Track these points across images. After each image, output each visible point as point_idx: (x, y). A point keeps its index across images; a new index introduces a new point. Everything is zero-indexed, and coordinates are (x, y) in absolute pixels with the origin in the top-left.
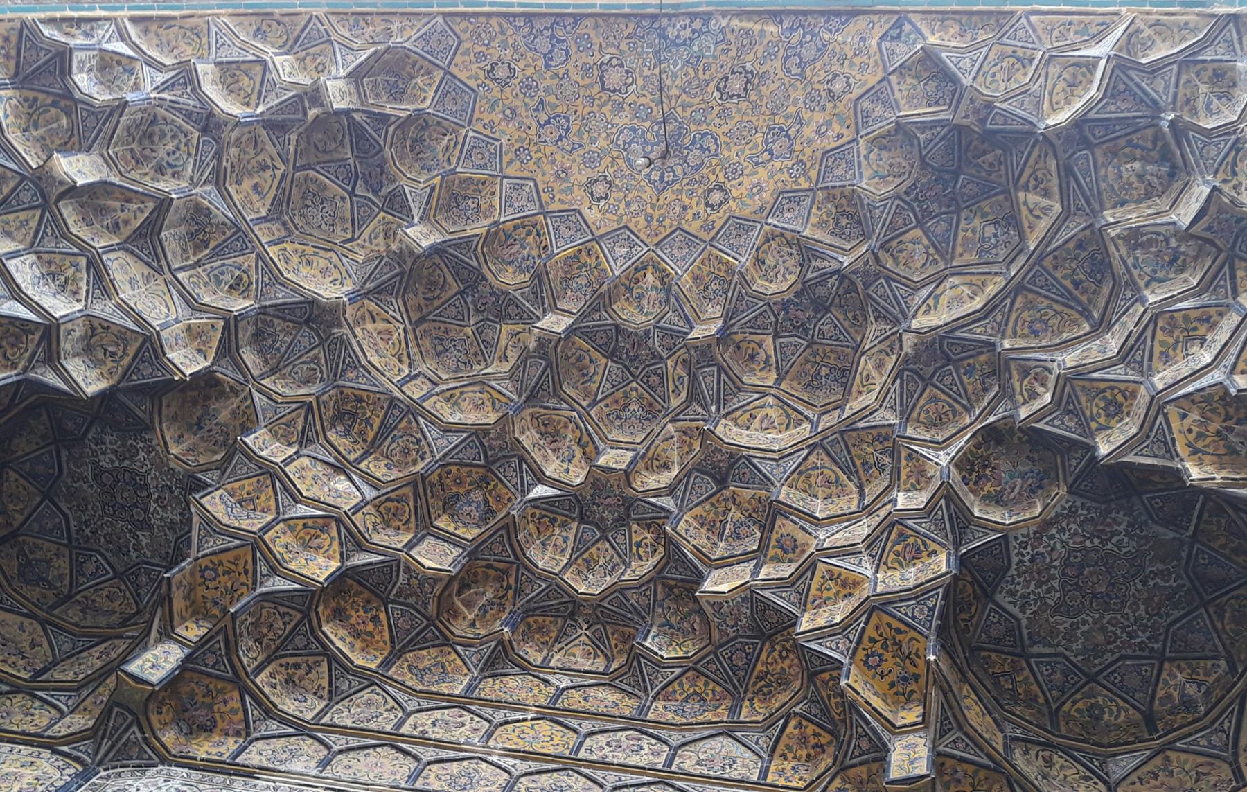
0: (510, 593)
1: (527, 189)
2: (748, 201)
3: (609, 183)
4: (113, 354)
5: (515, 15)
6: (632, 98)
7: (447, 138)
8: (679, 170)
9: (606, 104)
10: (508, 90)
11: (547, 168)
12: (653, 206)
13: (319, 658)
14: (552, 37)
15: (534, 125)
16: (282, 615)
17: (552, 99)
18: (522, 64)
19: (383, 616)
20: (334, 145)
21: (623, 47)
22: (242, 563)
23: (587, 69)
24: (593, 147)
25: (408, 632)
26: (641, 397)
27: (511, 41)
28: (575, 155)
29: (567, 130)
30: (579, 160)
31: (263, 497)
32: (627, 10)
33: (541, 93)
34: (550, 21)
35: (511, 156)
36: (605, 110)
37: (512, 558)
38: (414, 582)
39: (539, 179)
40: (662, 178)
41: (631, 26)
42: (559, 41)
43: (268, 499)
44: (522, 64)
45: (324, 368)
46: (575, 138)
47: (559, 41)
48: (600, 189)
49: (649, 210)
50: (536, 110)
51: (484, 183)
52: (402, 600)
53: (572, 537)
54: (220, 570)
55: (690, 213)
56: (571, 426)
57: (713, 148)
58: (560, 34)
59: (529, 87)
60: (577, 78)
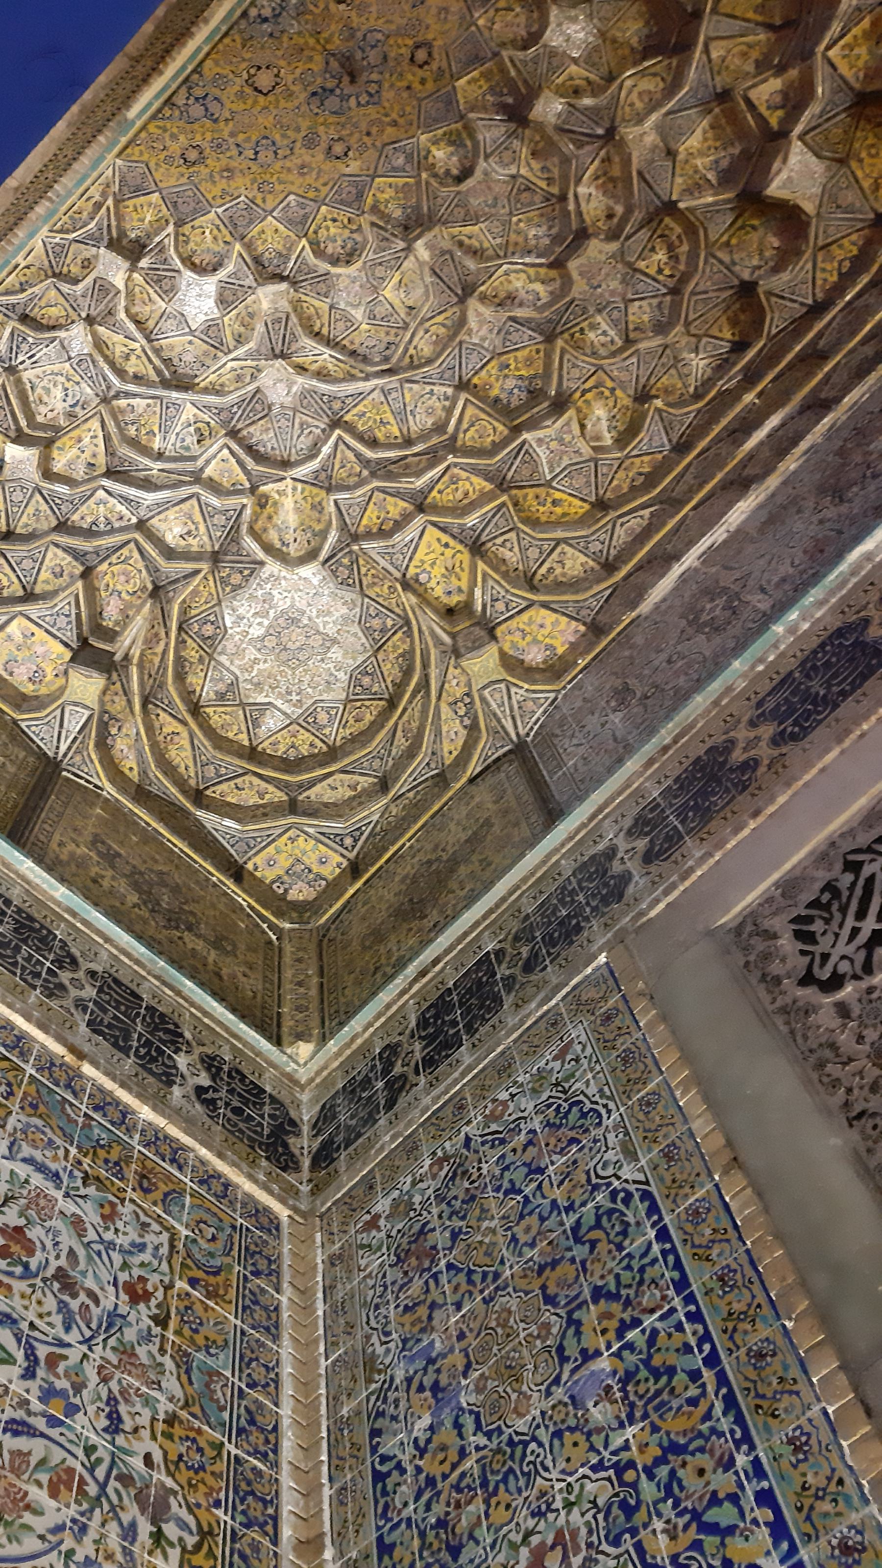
0: (619, 393)
1: (293, 204)
2: (447, 27)
3: (340, 139)
4: (189, 533)
5: (159, 111)
6: (290, 78)
7: (207, 232)
8: (375, 76)
9: (277, 101)
10: (208, 162)
11: (291, 177)
12: (386, 115)
13: (559, 550)
14: (197, 99)
15: (251, 164)
16: (503, 545)
17: (241, 137)
18: (198, 137)
19: (558, 495)
20: (148, 308)
21: (248, 56)
22: (436, 545)
23: (241, 95)
24: (303, 134)
25: (588, 483)
26: (529, 220)
27: (175, 130)
28: (296, 151)
29: (274, 143)
30: (303, 151)
31: (390, 508)
32: (224, 28)
33: (231, 140)
34: (184, 90)
35: (260, 195)
36: (282, 104)
37: (593, 369)
38: (554, 445)
39: (293, 188)
40: (371, 95)
41: (237, 38)
42: (204, 98)
43: (396, 505)
44: (198, 137)
45: (316, 423)
46: (285, 142)
47: (204, 98)
48: (338, 149)
49: (388, 119)
50: (240, 153)
51: (263, 232)
52: (558, 470)
53: (606, 328)
54: (427, 566)
55: (417, 86)
56: (513, 276)
57: (379, 36)
58: (198, 92)
59: (219, 146)
60: (242, 106)
